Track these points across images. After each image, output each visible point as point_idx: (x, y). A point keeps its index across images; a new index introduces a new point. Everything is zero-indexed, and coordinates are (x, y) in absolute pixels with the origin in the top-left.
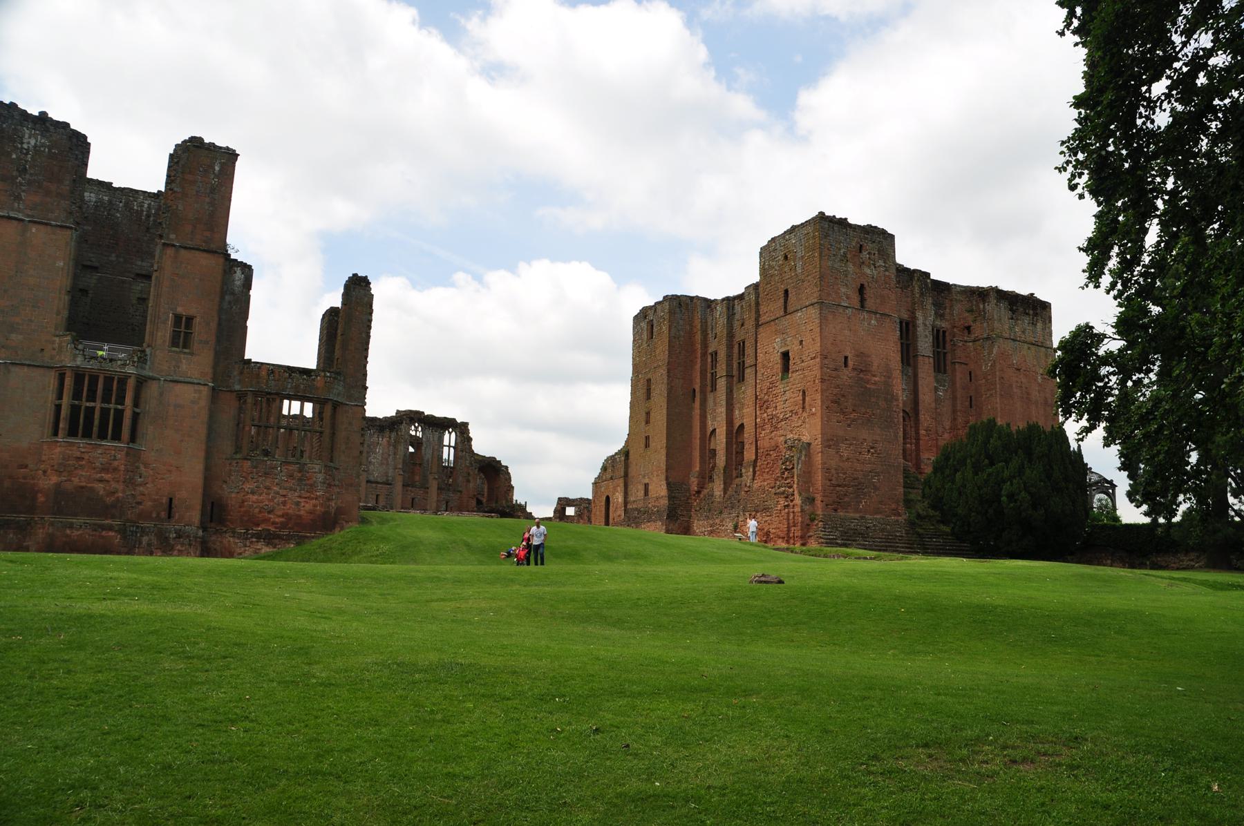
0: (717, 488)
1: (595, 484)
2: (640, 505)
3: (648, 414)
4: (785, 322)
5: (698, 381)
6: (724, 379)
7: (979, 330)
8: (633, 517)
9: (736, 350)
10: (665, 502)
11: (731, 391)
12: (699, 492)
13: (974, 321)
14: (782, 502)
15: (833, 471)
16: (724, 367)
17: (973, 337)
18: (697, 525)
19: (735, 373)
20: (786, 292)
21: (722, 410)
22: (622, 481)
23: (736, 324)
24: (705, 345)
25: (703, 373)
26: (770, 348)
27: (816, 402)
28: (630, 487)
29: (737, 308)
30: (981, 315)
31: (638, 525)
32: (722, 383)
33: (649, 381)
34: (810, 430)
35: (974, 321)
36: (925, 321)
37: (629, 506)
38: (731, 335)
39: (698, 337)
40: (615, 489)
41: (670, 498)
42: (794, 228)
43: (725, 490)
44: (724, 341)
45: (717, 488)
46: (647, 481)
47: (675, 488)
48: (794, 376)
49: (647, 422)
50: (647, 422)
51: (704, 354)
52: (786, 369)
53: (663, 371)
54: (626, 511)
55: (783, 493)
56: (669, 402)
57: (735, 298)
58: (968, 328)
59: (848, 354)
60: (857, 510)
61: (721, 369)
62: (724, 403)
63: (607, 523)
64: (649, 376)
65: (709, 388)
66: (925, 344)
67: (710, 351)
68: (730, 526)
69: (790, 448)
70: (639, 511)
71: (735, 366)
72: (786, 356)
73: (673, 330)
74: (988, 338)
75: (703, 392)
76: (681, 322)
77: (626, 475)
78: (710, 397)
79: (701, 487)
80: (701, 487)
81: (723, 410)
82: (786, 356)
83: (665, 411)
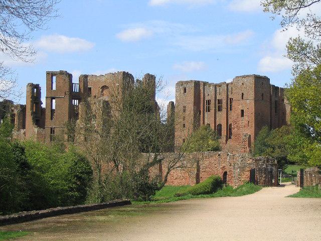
4: (242, 101)
16: (213, 106)
20: (243, 93)
24: (204, 98)
26: (237, 106)
29: (218, 89)
34: (250, 131)
36: (274, 99)
38: (216, 97)
42: (244, 77)
48: (246, 118)
51: (204, 100)
52: (242, 115)
61: (212, 106)
66: (273, 106)
72: (242, 111)
82: (242, 111)
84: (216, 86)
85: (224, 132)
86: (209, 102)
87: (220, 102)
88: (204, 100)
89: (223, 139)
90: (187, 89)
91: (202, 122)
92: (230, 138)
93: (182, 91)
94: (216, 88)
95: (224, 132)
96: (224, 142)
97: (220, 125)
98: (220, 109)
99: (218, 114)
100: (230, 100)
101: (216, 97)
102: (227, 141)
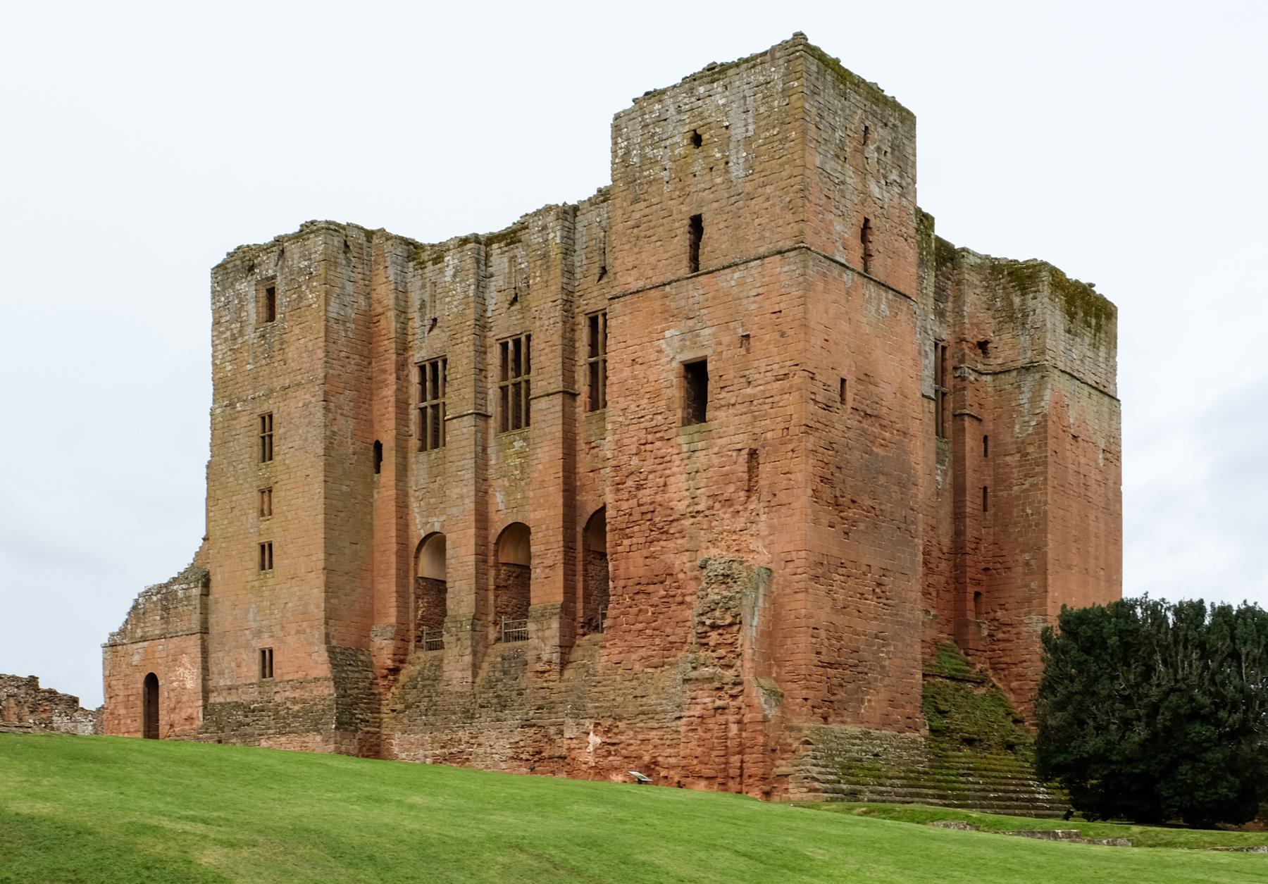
0: (456, 666)
1: (112, 646)
2: (250, 696)
3: (267, 492)
5: (390, 424)
6: (468, 421)
7: (1007, 349)
8: (225, 721)
9: (494, 357)
10: (328, 691)
11: (484, 449)
12: (395, 671)
13: (998, 332)
14: (706, 699)
15: (823, 634)
16: (468, 393)
17: (995, 362)
18: (396, 742)
19: (493, 408)
21: (462, 493)
22: (193, 644)
23: (495, 300)
24: (403, 347)
25: (402, 407)
26: (646, 358)
27: (795, 473)
28: (214, 656)
30: (1013, 318)
31: (247, 739)
32: (460, 432)
33: (267, 420)
34: (776, 538)
35: (998, 332)
37: (215, 698)
38: (482, 325)
39: (389, 324)
40: (175, 660)
41: (338, 682)
43: (475, 667)
44: (467, 336)
45: (456, 666)
46: (267, 643)
47: (347, 658)
49: (265, 512)
50: (265, 512)
51: (402, 366)
53: (311, 397)
54: (205, 707)
55: (710, 680)
56: (328, 468)
57: (491, 239)
58: (983, 346)
59: (844, 374)
60: (858, 719)
62: (469, 475)
63: (151, 729)
64: (266, 407)
65: (414, 442)
67: (419, 355)
68: (503, 747)
69: (726, 578)
70: (247, 709)
71: (493, 393)
72: (696, 373)
73: (334, 307)
74: (1027, 369)
75: (402, 451)
76: (350, 288)
77: (205, 630)
78: (420, 465)
79: (401, 658)
80: (401, 658)
81: (469, 491)
82: (696, 373)
83: (318, 489)
84: (480, 247)
85: (547, 587)
86: (434, 373)
87: (517, 355)
88: (402, 366)
89: (543, 638)
90: (280, 288)
91: (412, 573)
92: (593, 625)
93: (252, 312)
94: (483, 261)
95: (547, 587)
96: (549, 651)
97: (518, 533)
98: (517, 413)
99: (505, 453)
100: (593, 321)
101: (482, 325)
102: (566, 647)
